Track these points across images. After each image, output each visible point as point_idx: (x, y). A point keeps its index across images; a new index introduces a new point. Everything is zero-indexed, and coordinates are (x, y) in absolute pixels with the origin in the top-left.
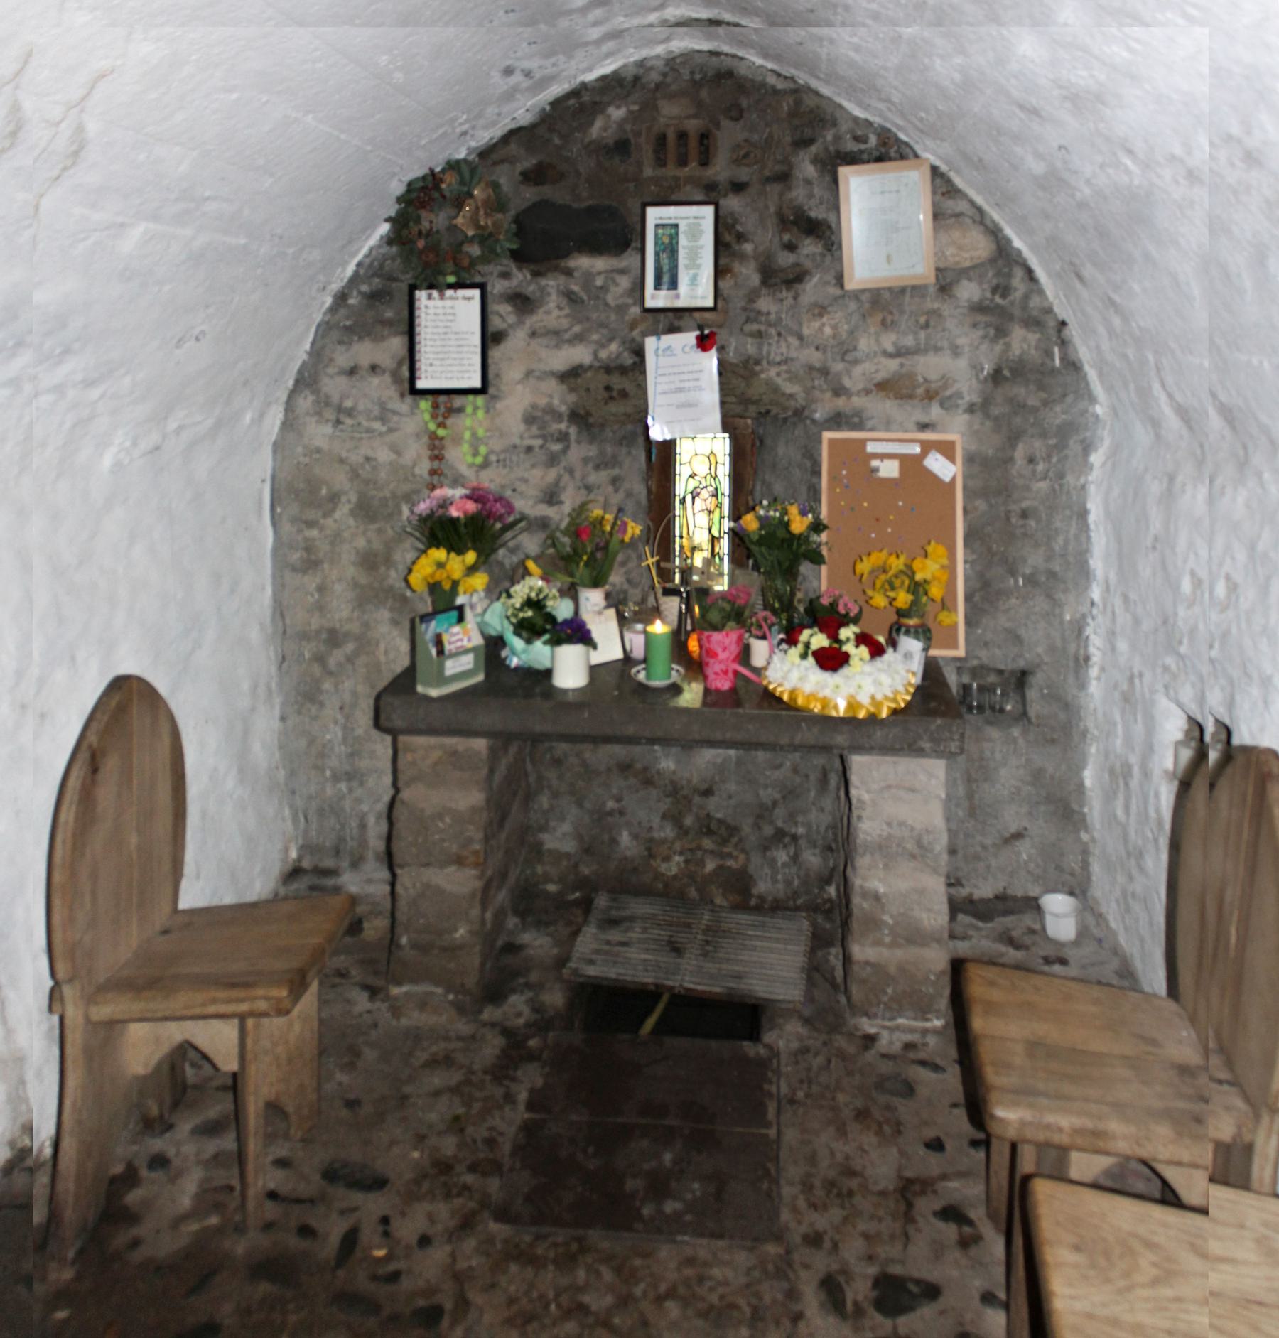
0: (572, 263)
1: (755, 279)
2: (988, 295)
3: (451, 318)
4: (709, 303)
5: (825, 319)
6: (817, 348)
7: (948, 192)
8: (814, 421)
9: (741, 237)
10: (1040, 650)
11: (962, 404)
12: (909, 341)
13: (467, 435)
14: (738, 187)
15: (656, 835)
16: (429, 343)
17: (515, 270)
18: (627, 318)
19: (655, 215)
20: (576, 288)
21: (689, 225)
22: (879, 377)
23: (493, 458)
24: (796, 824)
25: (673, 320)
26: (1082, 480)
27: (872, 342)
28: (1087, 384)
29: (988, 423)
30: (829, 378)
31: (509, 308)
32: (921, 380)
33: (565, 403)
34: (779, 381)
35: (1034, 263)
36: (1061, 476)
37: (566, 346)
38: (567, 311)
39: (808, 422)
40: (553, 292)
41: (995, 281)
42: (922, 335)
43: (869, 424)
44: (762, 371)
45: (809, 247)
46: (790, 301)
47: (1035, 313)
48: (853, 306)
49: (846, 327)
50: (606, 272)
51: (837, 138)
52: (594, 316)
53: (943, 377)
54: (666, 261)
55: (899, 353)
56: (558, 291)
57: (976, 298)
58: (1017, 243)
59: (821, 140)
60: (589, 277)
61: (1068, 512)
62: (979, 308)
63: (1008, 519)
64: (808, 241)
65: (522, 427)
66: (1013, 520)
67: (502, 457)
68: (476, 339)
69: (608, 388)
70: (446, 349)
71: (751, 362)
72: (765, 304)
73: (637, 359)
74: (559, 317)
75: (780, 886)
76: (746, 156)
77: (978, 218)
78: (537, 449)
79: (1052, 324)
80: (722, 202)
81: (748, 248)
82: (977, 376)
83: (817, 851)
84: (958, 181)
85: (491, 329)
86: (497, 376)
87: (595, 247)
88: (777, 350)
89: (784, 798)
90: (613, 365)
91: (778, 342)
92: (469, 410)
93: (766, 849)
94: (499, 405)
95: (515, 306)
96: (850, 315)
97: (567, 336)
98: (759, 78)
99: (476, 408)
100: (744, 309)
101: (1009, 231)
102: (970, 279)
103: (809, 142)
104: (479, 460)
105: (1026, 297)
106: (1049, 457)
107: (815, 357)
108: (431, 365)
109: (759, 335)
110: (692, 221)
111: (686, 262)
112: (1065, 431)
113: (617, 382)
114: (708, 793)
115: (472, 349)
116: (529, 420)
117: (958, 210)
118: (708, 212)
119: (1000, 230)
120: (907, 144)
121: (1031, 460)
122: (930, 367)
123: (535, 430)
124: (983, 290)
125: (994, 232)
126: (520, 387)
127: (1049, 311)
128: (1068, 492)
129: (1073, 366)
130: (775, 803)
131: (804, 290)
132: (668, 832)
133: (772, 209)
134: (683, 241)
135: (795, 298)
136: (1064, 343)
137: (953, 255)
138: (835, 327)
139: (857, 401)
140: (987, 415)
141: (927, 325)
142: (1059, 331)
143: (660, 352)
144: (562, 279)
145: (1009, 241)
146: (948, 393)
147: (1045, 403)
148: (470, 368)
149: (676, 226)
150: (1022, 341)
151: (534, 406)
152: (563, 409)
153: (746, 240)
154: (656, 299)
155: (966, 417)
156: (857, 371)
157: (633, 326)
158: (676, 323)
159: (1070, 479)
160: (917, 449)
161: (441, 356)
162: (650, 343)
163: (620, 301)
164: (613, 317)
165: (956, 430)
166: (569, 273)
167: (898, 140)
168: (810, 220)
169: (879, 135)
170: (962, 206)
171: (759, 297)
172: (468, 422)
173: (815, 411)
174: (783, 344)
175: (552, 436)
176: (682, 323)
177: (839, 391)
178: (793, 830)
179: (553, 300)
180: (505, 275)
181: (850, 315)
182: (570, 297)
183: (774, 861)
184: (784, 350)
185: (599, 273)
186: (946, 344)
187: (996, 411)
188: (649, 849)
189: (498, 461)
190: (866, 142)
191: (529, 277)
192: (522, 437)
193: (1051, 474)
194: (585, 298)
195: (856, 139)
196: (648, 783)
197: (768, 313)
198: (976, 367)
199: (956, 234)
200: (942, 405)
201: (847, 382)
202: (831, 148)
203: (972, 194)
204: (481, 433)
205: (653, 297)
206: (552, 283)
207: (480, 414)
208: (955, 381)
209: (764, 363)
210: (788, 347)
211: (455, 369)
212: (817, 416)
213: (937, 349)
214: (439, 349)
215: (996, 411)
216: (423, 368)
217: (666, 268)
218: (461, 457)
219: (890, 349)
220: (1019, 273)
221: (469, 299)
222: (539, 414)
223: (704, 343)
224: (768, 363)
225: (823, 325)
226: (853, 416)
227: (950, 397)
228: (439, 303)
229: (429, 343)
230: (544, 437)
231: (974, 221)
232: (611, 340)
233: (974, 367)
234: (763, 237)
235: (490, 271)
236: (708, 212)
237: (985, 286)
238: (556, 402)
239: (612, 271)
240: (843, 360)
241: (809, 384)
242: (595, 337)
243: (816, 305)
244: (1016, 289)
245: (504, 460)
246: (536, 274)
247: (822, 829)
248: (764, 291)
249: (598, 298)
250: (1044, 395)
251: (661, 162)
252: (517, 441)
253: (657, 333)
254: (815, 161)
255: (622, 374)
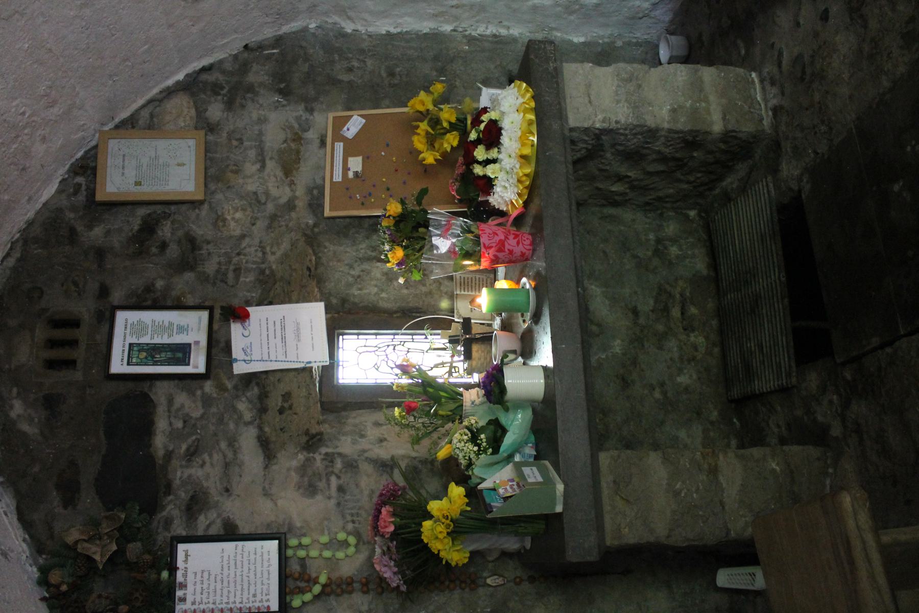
0: (161, 453)
1: (189, 276)
2: (220, 98)
3: (206, 575)
4: (205, 314)
5: (229, 218)
6: (253, 224)
7: (132, 124)
8: (315, 225)
9: (149, 289)
10: (492, 66)
11: (305, 116)
12: (252, 154)
13: (327, 554)
14: (104, 292)
15: (676, 355)
16: (232, 600)
17: (164, 513)
18: (215, 395)
19: (118, 365)
20: (184, 447)
21: (132, 334)
22: (280, 173)
23: (350, 526)
24: (648, 240)
25: (219, 347)
26: (365, 37)
27: (250, 180)
28: (294, 33)
29: (321, 99)
30: (279, 214)
31: (202, 518)
32: (285, 145)
33: (297, 454)
34: (279, 254)
35: (197, 65)
36: (362, 51)
37: (240, 456)
38: (206, 456)
39: (316, 230)
40: (188, 472)
41: (209, 93)
42: (246, 143)
43: (319, 182)
44: (270, 268)
45: (165, 231)
46: (210, 247)
47: (237, 67)
48: (219, 196)
49: (236, 201)
50: (169, 417)
51: (73, 208)
52: (212, 428)
53: (284, 130)
54: (163, 355)
55: (262, 161)
56: (187, 467)
57: (222, 106)
58: (180, 76)
59: (72, 221)
60: (175, 435)
61: (390, 47)
62: (229, 105)
63: (395, 85)
64: (160, 233)
65: (319, 497)
66: (396, 82)
67: (349, 518)
68: (229, 546)
69: (281, 411)
70: (239, 579)
71: (261, 278)
72: (210, 267)
73: (254, 383)
74: (212, 464)
75: (696, 251)
76: (76, 284)
77: (157, 103)
78: (341, 482)
79: (246, 55)
80: (116, 303)
81: (160, 284)
82: (283, 106)
83: (665, 224)
84: (125, 114)
85: (222, 532)
86: (268, 525)
87: (147, 429)
88: (252, 254)
89: (629, 250)
90: (258, 405)
91: (245, 255)
92: (302, 553)
93: (670, 263)
94: (298, 525)
95: (200, 511)
96: (226, 198)
97: (230, 455)
98: (8, 272)
99: (300, 546)
100: (214, 284)
101: (170, 82)
102: (206, 110)
103: (73, 231)
104: (352, 540)
105: (223, 72)
106: (347, 59)
107: (261, 224)
108: (254, 596)
109: (237, 270)
110: (128, 331)
111: (166, 336)
112: (328, 48)
113: (275, 401)
114: (635, 312)
115: (240, 548)
116: (311, 490)
117: (147, 116)
118: (121, 317)
119: (168, 88)
120: (86, 152)
121: (350, 70)
122: (274, 137)
123: (322, 485)
124: (216, 100)
125: (169, 93)
126: (280, 502)
127: (236, 57)
128: (374, 46)
129: (278, 41)
130: (635, 257)
131: (202, 235)
132: (672, 344)
133: (128, 263)
134: (146, 340)
135: (208, 243)
136: (261, 47)
137: (185, 121)
138: (236, 210)
139: (300, 191)
140: (316, 99)
141: (240, 140)
142: (252, 50)
143: (246, 358)
144: (175, 462)
145: (178, 83)
146: (296, 126)
147: (307, 59)
148: (259, 551)
149: (131, 345)
150: (258, 75)
151: (299, 487)
152: (301, 457)
153: (153, 285)
154: (198, 364)
155: (315, 114)
156: (274, 192)
157: (221, 388)
158: (222, 345)
159: (365, 45)
160: (339, 147)
161: (246, 587)
162: (239, 368)
163: (199, 404)
164: (214, 410)
165: (324, 119)
166: (169, 455)
167: (83, 158)
168: (141, 230)
169: (76, 174)
170: (145, 113)
171: (204, 273)
172: (314, 553)
173: (307, 224)
174: (248, 250)
175: (327, 467)
176: (223, 340)
177: (290, 206)
178: (653, 243)
179: (196, 472)
180: (168, 523)
181: (226, 198)
182: (192, 454)
183: (677, 257)
184: (253, 249)
185: (171, 424)
186: (256, 128)
187: (312, 93)
188: (689, 361)
189: (353, 522)
190: (80, 185)
191: (171, 497)
192: (329, 498)
193: (361, 58)
194: (194, 437)
195: (76, 193)
196: (634, 362)
197: (219, 263)
198: (277, 106)
199: (168, 118)
200: (306, 130)
201: (284, 200)
202: (81, 213)
203: (135, 106)
204: (324, 539)
205: (197, 367)
206: (179, 474)
207: (306, 541)
208: (287, 121)
209: (263, 266)
210: (250, 246)
211: (259, 569)
212: (311, 222)
213: (261, 134)
214: (239, 587)
215: (312, 93)
216: (257, 604)
217: (169, 355)
218: (350, 562)
219: (258, 166)
220: (204, 77)
221: (187, 556)
222: (306, 479)
223: (243, 316)
224: (263, 263)
225: (233, 219)
226: (312, 194)
227: (300, 125)
228: (190, 587)
229: (232, 600)
230: (328, 475)
231: (159, 106)
232: (235, 409)
233: (276, 108)
234: (152, 272)
235: (162, 537)
236: (121, 317)
237: (213, 99)
238: (294, 463)
239: (169, 411)
240: (265, 204)
241: (284, 228)
242: (232, 426)
243: (215, 224)
244: (217, 79)
245: (352, 515)
246: (169, 489)
247: (648, 221)
248: (200, 269)
249: (194, 425)
250: (300, 61)
251: (70, 364)
252: (333, 502)
253: (231, 362)
254: (90, 227)
255: (267, 397)
